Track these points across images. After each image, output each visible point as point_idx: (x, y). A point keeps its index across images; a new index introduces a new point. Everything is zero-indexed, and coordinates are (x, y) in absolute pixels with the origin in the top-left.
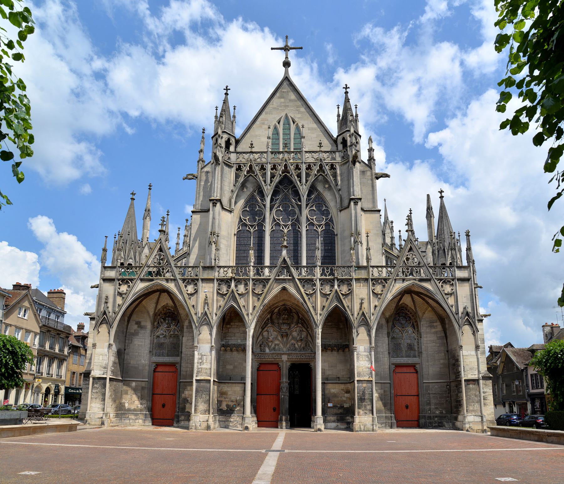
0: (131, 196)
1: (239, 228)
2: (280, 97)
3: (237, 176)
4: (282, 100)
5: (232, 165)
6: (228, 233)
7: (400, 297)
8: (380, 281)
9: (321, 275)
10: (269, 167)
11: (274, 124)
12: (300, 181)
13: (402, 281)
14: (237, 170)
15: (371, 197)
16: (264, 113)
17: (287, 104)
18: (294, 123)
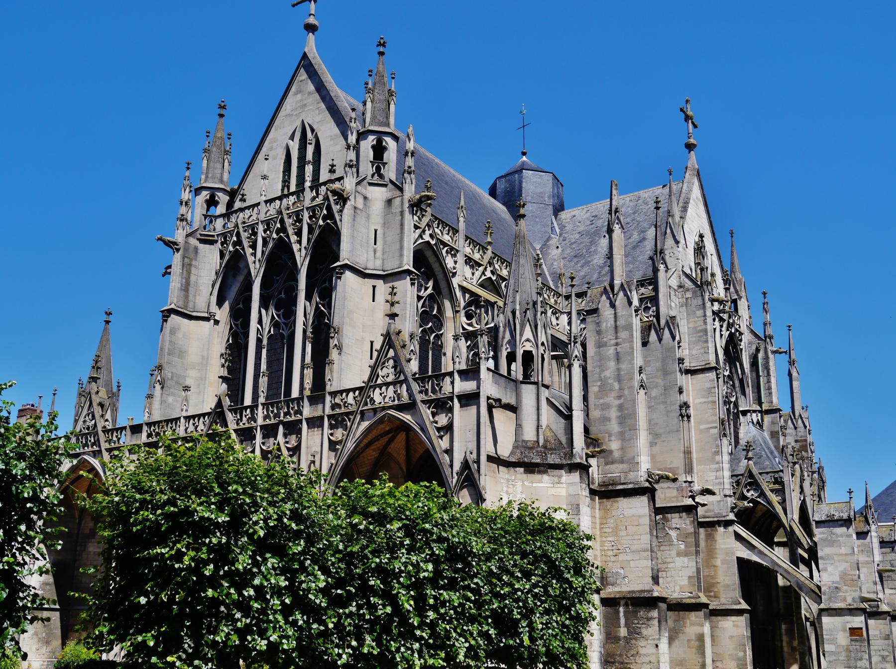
0: (105, 318)
1: (228, 340)
2: (296, 94)
3: (222, 255)
4: (299, 97)
5: (216, 238)
6: (203, 358)
7: (386, 438)
8: (340, 419)
9: (265, 420)
10: (261, 228)
11: (284, 145)
12: (300, 242)
13: (372, 414)
14: (222, 244)
15: (398, 247)
16: (273, 129)
17: (305, 102)
18: (313, 130)
